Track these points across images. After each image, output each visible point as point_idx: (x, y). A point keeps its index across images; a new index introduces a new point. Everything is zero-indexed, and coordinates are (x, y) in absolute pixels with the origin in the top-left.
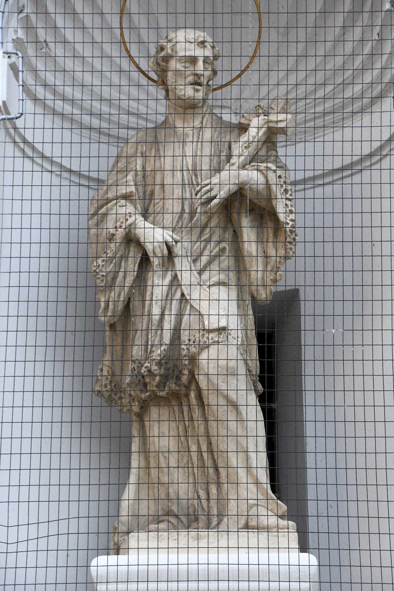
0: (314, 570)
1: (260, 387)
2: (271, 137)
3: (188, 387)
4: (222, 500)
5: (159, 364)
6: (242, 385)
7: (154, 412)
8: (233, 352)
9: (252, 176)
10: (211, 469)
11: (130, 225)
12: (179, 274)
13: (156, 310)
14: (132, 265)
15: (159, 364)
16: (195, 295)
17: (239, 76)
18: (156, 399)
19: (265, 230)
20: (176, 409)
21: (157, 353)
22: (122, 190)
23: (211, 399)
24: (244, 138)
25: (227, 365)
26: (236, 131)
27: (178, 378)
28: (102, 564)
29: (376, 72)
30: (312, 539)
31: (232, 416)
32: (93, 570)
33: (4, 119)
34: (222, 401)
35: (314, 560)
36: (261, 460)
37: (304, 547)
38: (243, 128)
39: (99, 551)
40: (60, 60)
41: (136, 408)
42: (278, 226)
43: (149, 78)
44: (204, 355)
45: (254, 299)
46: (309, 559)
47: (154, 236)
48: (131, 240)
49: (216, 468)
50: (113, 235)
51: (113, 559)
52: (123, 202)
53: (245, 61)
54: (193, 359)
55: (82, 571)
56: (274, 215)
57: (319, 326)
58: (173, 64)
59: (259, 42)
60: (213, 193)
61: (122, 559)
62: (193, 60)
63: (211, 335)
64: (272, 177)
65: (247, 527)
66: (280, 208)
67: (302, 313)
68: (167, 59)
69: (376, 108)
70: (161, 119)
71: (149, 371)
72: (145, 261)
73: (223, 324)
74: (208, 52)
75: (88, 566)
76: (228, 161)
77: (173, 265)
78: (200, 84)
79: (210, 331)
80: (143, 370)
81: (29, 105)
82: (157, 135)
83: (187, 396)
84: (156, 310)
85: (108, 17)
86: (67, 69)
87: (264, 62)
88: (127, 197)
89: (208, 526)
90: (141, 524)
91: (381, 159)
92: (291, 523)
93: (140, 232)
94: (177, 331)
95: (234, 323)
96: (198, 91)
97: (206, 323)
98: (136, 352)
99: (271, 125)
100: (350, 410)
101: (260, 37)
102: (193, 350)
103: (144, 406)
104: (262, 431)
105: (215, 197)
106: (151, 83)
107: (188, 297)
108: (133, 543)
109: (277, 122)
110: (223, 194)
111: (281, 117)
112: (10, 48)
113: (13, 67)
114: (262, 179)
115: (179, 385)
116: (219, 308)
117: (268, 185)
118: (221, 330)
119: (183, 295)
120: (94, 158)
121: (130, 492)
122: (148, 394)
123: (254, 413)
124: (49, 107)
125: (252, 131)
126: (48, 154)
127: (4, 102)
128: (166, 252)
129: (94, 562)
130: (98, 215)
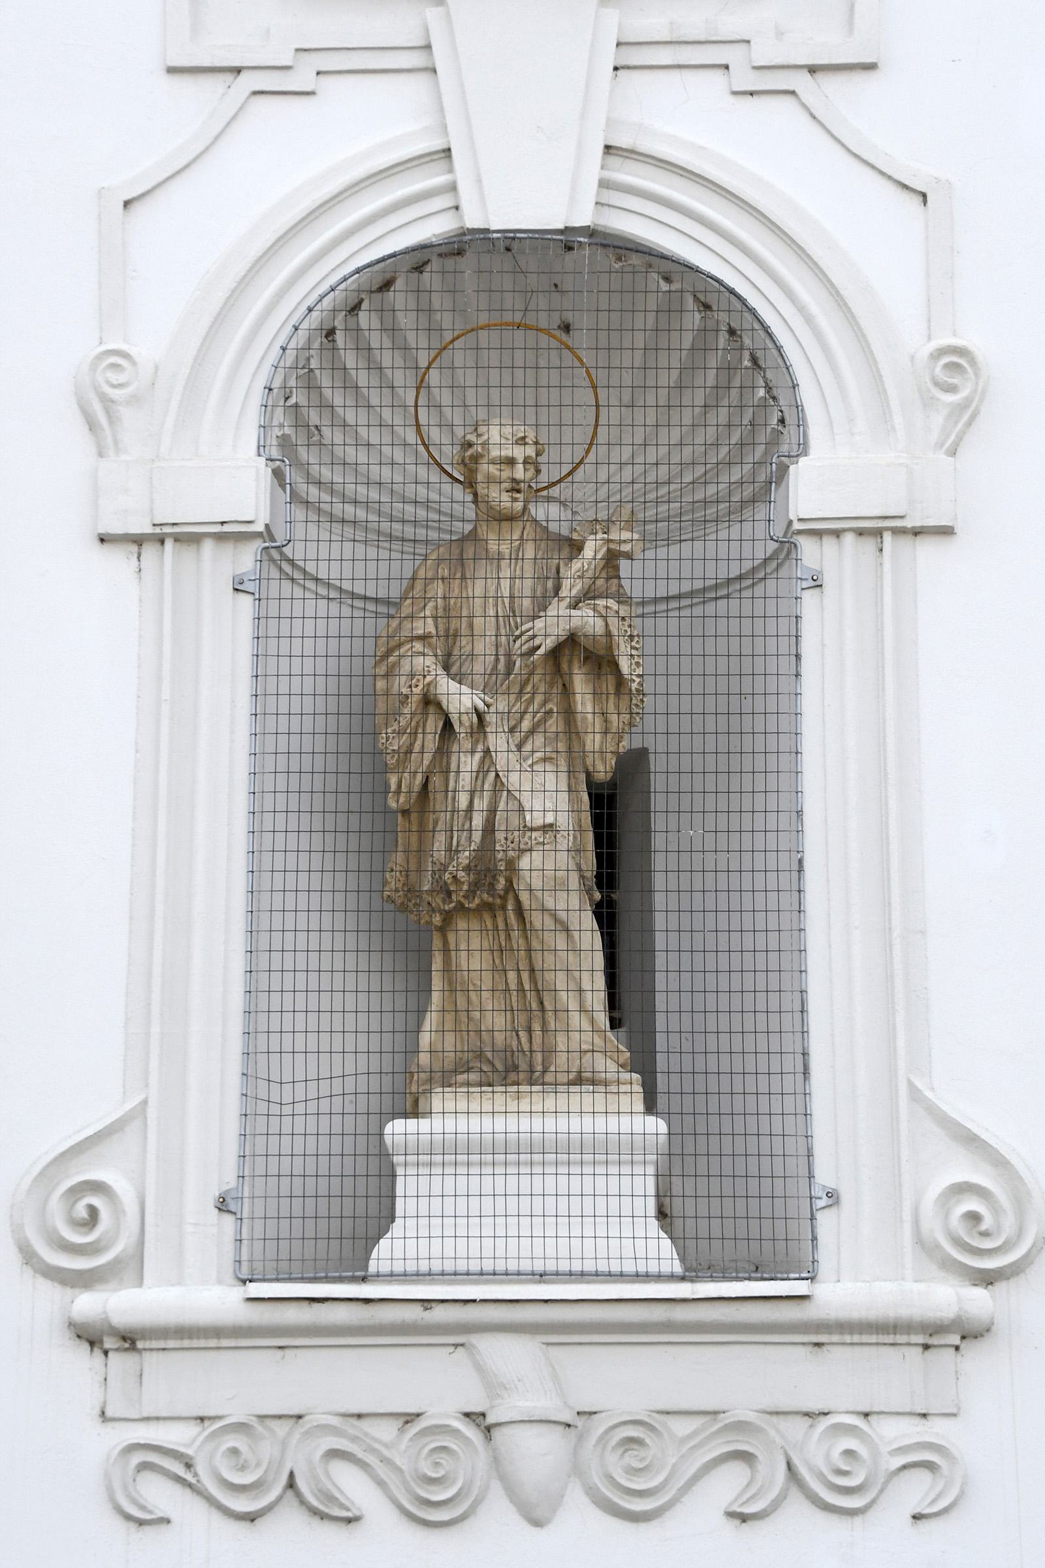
0: (663, 1139)
1: (597, 896)
2: (612, 559)
3: (504, 898)
4: (549, 1052)
5: (467, 869)
6: (575, 902)
7: (462, 924)
8: (563, 859)
9: (587, 620)
10: (534, 1001)
11: (429, 684)
13: (463, 800)
15: (467, 869)
17: (570, 473)
19: (603, 678)
21: (464, 858)
22: (419, 628)
23: (536, 919)
24: (576, 565)
25: (554, 873)
26: (566, 552)
27: (492, 885)
28: (397, 1129)
29: (747, 468)
30: (662, 1101)
31: (561, 944)
32: (388, 1140)
33: (267, 548)
34: (549, 923)
35: (663, 1127)
36: (598, 1000)
37: (650, 1107)
38: (577, 547)
39: (394, 1116)
40: (338, 451)
41: (437, 919)
42: (620, 681)
45: (588, 774)
46: (656, 1125)
47: (460, 699)
48: (429, 701)
50: (407, 696)
51: (412, 1123)
52: (418, 646)
53: (579, 452)
54: (512, 866)
55: (374, 1140)
56: (615, 665)
57: (673, 826)
58: (484, 468)
59: (596, 425)
60: (537, 642)
61: (424, 1124)
62: (511, 462)
63: (534, 834)
64: (613, 622)
66: (625, 665)
67: (652, 770)
68: (476, 458)
69: (747, 514)
70: (469, 527)
71: (455, 877)
72: (448, 725)
73: (550, 819)
74: (531, 451)
75: (381, 1135)
76: (556, 594)
78: (518, 491)
79: (532, 829)
80: (447, 875)
81: (300, 514)
82: (463, 553)
83: (503, 908)
84: (463, 800)
85: (401, 391)
86: (348, 460)
87: (603, 450)
88: (423, 638)
90: (447, 1077)
91: (753, 585)
92: (635, 1076)
94: (489, 829)
95: (564, 821)
96: (515, 500)
97: (528, 817)
98: (440, 843)
99: (612, 546)
100: (710, 937)
101: (597, 421)
102: (511, 853)
103: (448, 917)
104: (599, 960)
105: (539, 647)
108: (437, 1105)
109: (621, 542)
110: (550, 643)
111: (626, 535)
112: (275, 453)
113: (278, 474)
115: (493, 896)
116: (547, 798)
118: (547, 828)
120: (377, 571)
121: (431, 1021)
122: (453, 905)
123: (590, 938)
124: (325, 512)
125: (588, 552)
126: (322, 575)
127: (267, 526)
128: (475, 719)
129: (388, 1129)
130: (387, 653)
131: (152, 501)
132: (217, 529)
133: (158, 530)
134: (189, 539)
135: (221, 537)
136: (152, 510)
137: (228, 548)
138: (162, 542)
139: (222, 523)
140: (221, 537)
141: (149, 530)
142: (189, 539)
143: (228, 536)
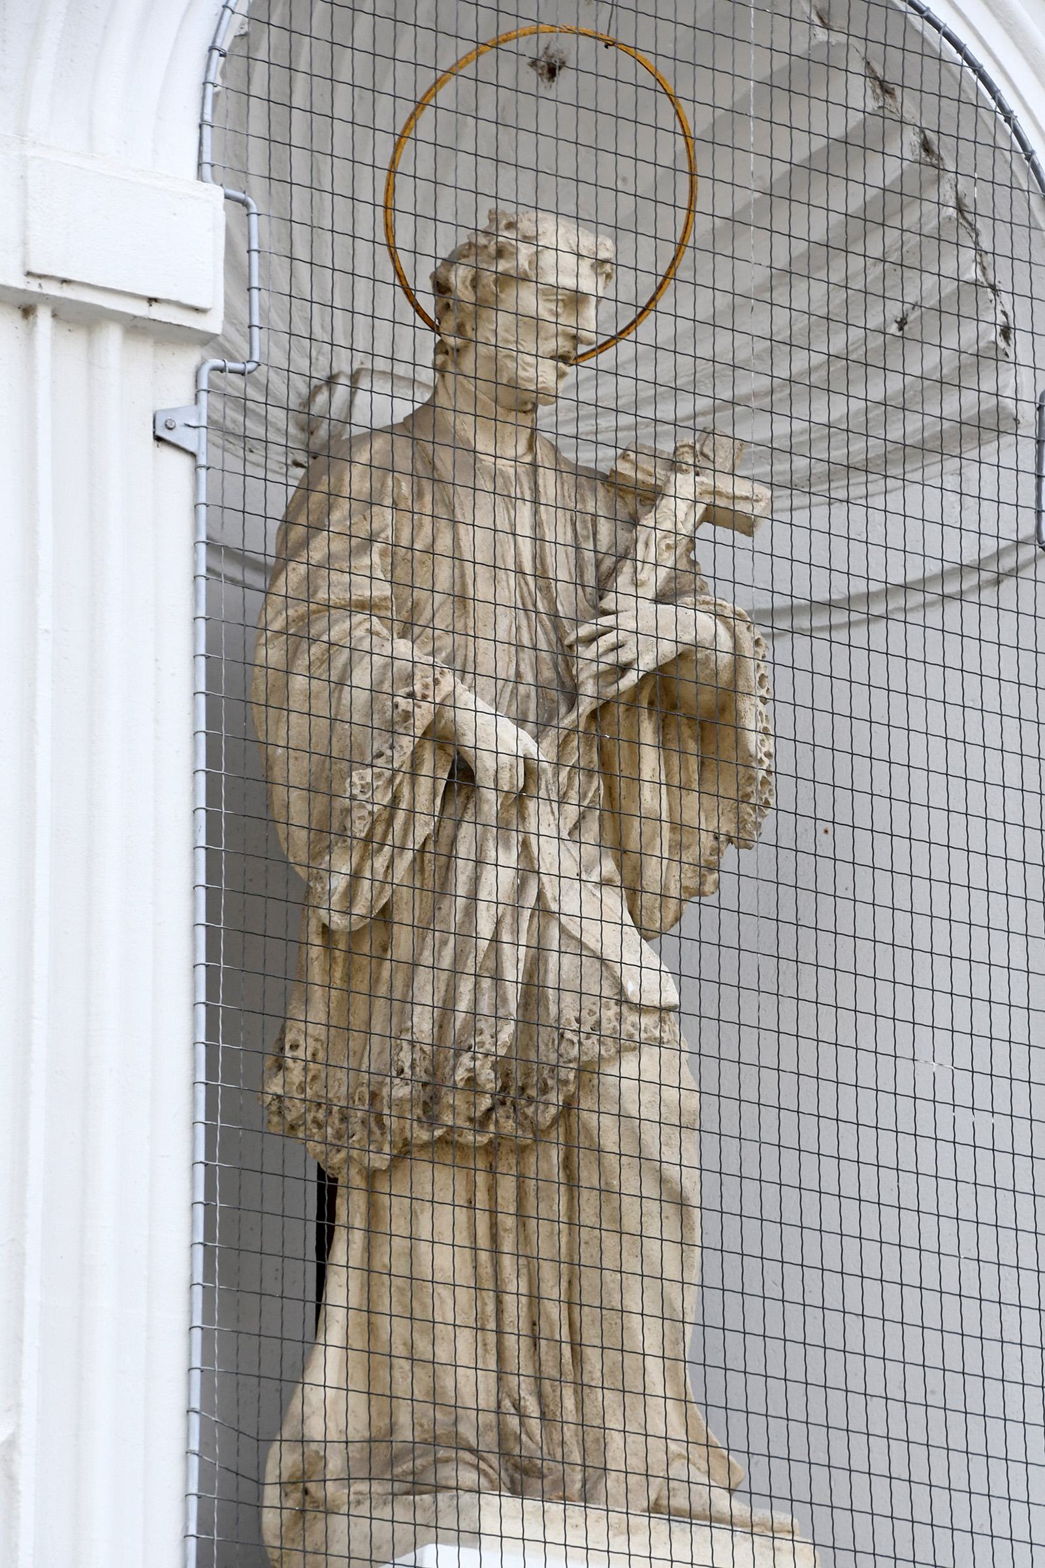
12: (533, 839)
14: (425, 794)
16: (570, 905)
18: (447, 1145)
20: (481, 1179)
43: (418, 309)
44: (629, 1066)
49: (577, 1347)
54: (588, 1071)
60: (625, 655)
62: (576, 299)
65: (654, 1509)
77: (522, 816)
79: (640, 1009)
89: (586, 1497)
93: (465, 719)
106: (420, 322)
107: (554, 907)
110: (647, 662)
114: (725, 641)
117: (737, 654)
119: (540, 896)
131: (25, 224)
132: (140, 309)
133: (33, 286)
134: (81, 318)
135: (135, 327)
136: (25, 243)
137: (145, 352)
138: (27, 311)
139: (152, 300)
140: (135, 327)
141: (18, 282)
142: (81, 318)
143: (150, 330)
